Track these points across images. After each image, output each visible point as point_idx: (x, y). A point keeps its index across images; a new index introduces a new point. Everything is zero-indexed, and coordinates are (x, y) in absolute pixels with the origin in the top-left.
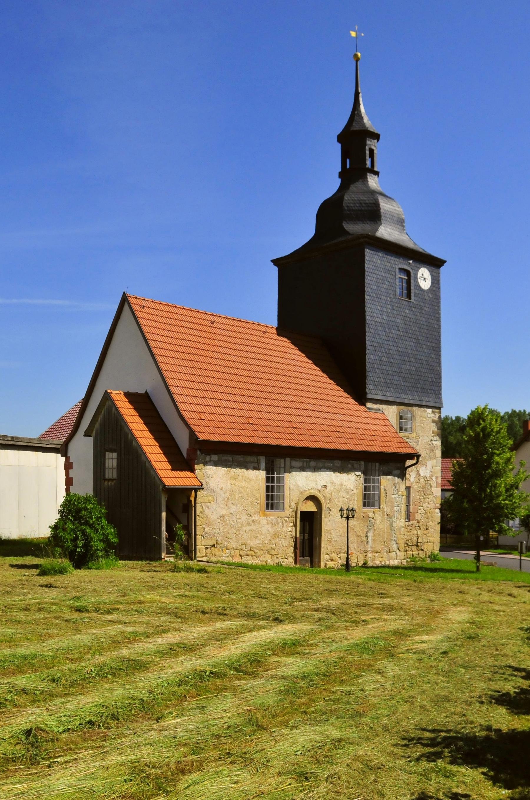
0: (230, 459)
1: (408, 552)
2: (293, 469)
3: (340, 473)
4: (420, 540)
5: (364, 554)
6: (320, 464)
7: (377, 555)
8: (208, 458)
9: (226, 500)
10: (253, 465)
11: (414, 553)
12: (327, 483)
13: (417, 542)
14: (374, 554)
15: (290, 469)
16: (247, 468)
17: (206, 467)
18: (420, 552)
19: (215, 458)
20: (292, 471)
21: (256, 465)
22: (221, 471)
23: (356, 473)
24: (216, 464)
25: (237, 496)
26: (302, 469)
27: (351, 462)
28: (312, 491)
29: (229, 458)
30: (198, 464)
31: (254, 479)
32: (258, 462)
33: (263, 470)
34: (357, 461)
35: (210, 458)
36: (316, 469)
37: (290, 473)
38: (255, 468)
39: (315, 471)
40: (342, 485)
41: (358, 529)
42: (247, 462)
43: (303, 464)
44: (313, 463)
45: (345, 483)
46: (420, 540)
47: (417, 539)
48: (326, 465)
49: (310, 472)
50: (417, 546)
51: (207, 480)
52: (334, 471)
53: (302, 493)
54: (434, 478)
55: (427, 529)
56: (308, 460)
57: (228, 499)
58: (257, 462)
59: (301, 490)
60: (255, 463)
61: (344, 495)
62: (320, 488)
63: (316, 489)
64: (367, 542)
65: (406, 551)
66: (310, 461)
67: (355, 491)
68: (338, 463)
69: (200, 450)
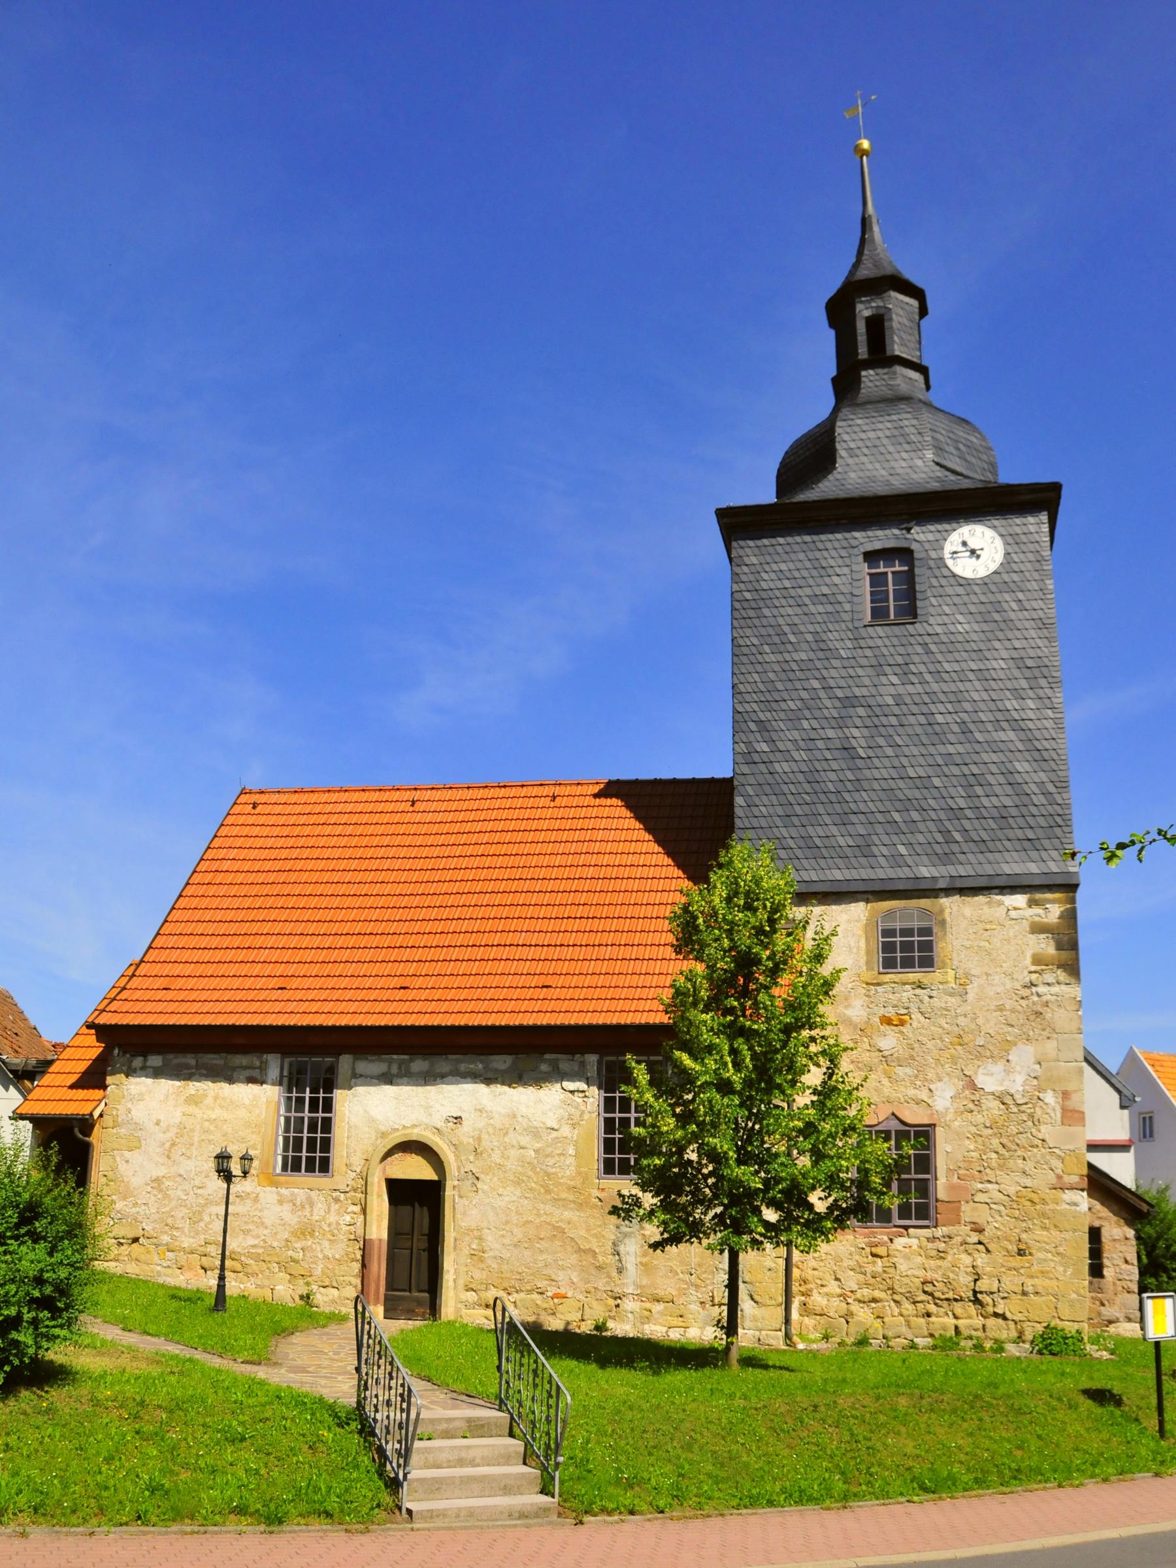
0: (193, 1062)
1: (933, 1319)
2: (359, 1081)
3: (510, 1086)
4: (982, 1285)
5: (612, 1302)
6: (443, 1065)
7: (658, 1308)
8: (138, 1062)
9: (168, 1145)
10: (248, 1073)
11: (960, 1323)
12: (461, 1109)
13: (975, 1292)
14: (648, 1305)
15: (357, 1078)
16: (231, 1080)
17: (131, 1079)
18: (992, 1322)
19: (155, 1060)
20: (356, 1085)
21: (256, 1073)
22: (166, 1086)
23: (566, 1084)
24: (157, 1073)
25: (196, 1139)
26: (387, 1079)
27: (547, 1056)
28: (415, 1131)
29: (190, 1060)
30: (113, 1073)
31: (247, 1102)
32: (263, 1068)
33: (273, 1084)
34: (573, 1054)
35: (145, 1061)
36: (429, 1078)
37: (350, 1088)
38: (251, 1080)
39: (426, 1084)
40: (515, 1116)
41: (583, 1233)
42: (234, 1069)
43: (389, 1068)
44: (419, 1065)
45: (524, 1110)
46: (982, 1285)
47: (976, 1280)
48: (463, 1067)
49: (408, 1084)
50: (977, 1301)
51: (129, 1105)
52: (488, 1081)
53: (383, 1135)
54: (1049, 1098)
55: (1021, 1253)
56: (406, 1057)
57: (173, 1145)
58: (260, 1068)
59: (383, 1128)
60: (255, 1068)
61: (525, 1140)
62: (440, 1124)
63: (427, 1127)
64: (620, 1271)
65: (929, 1315)
66: (411, 1060)
67: (566, 1131)
68: (502, 1062)
69: (120, 1047)
